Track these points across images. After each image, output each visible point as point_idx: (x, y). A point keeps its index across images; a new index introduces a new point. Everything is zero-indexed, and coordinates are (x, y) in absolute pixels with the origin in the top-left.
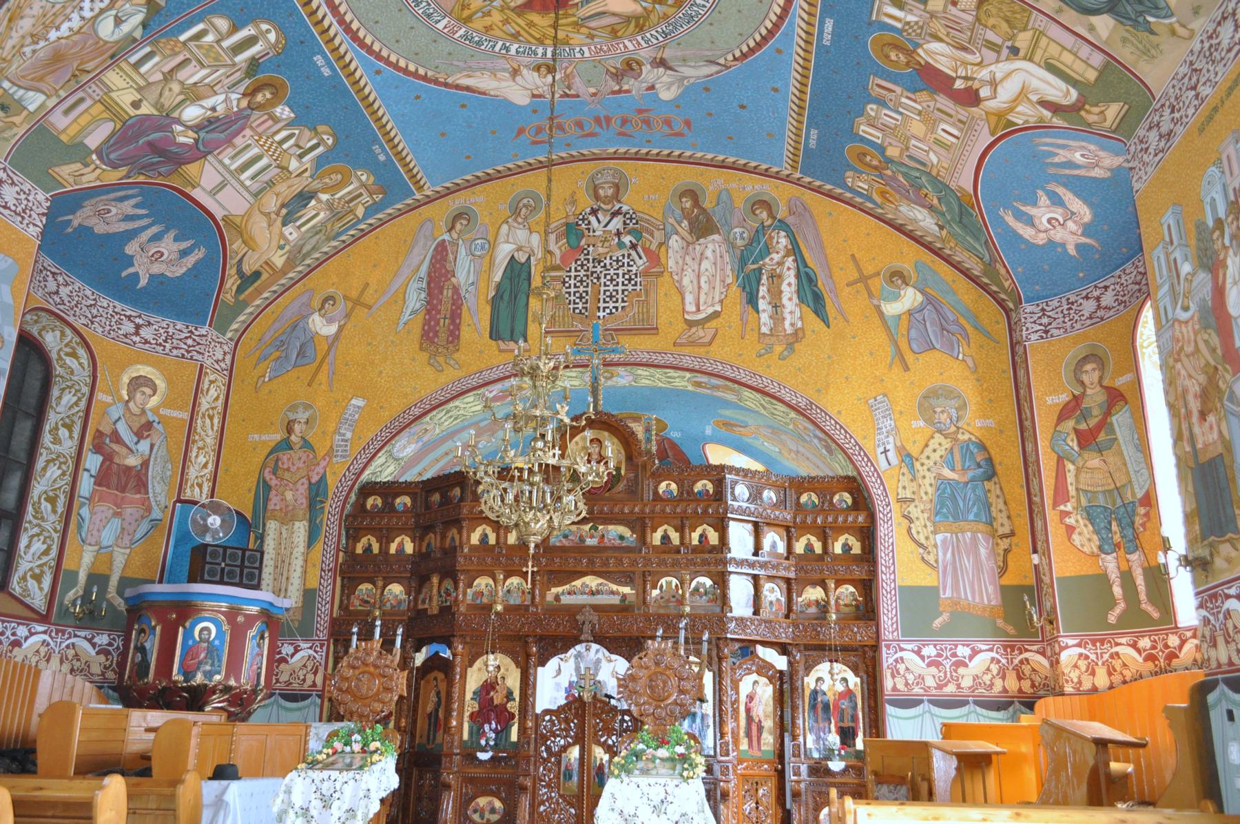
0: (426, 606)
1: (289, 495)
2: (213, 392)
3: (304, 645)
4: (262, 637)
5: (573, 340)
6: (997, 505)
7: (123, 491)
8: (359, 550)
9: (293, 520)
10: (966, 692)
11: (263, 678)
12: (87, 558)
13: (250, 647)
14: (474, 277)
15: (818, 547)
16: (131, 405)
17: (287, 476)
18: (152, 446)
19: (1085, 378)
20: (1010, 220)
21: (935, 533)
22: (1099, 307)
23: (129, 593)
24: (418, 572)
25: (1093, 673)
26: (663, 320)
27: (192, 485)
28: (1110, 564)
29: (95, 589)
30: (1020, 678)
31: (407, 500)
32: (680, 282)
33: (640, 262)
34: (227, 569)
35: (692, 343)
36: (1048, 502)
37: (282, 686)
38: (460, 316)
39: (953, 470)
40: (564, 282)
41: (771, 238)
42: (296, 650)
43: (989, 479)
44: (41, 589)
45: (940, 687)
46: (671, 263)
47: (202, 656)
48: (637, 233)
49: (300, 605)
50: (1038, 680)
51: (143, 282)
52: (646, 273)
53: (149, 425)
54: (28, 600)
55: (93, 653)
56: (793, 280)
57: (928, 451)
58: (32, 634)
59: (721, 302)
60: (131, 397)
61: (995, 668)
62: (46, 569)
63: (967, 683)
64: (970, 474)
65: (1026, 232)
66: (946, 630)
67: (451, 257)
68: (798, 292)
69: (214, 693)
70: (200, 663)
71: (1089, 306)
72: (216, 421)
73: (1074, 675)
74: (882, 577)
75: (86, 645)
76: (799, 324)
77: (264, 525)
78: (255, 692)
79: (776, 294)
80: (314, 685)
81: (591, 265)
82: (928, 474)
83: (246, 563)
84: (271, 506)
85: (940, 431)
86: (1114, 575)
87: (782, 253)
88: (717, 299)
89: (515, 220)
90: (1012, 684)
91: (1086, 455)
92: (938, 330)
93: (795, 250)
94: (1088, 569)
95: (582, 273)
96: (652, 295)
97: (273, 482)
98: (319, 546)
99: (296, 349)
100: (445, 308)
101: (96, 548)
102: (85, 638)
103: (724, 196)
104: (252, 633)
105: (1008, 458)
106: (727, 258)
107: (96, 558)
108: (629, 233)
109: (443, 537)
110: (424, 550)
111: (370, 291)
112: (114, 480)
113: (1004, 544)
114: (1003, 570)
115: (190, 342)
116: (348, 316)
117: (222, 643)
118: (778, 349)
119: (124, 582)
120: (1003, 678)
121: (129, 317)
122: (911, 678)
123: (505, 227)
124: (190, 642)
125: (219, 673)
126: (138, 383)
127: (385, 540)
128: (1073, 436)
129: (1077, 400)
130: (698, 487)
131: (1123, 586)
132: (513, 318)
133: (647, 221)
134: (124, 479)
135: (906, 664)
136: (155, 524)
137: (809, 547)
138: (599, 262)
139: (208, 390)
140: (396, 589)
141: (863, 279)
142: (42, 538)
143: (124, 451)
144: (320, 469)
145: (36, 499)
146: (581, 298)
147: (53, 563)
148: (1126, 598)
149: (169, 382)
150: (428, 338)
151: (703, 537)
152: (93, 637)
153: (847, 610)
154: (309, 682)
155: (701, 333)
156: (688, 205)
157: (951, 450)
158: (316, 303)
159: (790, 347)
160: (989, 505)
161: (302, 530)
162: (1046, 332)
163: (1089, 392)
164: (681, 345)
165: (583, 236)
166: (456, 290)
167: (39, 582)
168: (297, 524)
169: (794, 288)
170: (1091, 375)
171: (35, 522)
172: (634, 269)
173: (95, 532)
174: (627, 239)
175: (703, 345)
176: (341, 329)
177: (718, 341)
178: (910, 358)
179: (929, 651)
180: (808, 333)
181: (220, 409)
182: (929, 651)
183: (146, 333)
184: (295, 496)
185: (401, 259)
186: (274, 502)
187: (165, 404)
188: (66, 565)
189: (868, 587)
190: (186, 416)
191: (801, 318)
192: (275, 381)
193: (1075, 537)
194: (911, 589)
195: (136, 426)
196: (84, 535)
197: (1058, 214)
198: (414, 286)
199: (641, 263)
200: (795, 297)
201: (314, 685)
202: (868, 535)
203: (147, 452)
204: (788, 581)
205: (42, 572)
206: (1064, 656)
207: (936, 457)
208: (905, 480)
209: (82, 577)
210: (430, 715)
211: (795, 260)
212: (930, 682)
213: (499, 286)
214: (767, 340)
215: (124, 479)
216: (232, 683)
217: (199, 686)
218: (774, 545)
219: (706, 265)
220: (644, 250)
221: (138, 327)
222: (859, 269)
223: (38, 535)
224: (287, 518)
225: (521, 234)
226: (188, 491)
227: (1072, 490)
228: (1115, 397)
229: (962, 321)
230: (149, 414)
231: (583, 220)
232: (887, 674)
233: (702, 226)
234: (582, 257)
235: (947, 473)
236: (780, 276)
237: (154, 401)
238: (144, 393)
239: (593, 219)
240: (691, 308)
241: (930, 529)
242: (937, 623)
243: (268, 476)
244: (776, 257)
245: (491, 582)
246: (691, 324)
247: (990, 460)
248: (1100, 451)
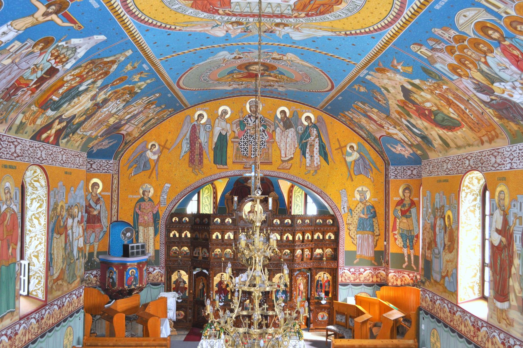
0: (197, 255)
1: (146, 218)
2: (115, 182)
3: (156, 268)
5: (243, 166)
6: (376, 226)
8: (171, 236)
9: (148, 226)
10: (362, 282)
14: (207, 141)
15: (321, 237)
17: (144, 211)
18: (101, 206)
19: (405, 194)
20: (389, 146)
21: (357, 234)
22: (412, 174)
23: (101, 257)
24: (193, 243)
25: (397, 281)
26: (274, 159)
28: (405, 251)
30: (377, 278)
31: (187, 219)
32: (280, 145)
33: (266, 137)
35: (283, 169)
36: (390, 230)
38: (202, 154)
39: (364, 214)
40: (239, 144)
41: (311, 131)
42: (154, 270)
43: (374, 217)
45: (354, 280)
46: (277, 138)
48: (264, 126)
50: (382, 278)
51: (94, 152)
52: (268, 142)
56: (318, 147)
57: (357, 208)
59: (294, 154)
61: (370, 275)
63: (362, 279)
64: (369, 216)
65: (394, 150)
66: (357, 264)
67: (198, 131)
68: (319, 152)
71: (409, 172)
73: (392, 281)
74: (340, 248)
76: (319, 163)
79: (312, 152)
80: (162, 280)
81: (249, 137)
82: (356, 216)
84: (140, 221)
85: (361, 202)
86: (406, 254)
87: (315, 137)
88: (292, 153)
89: (221, 118)
90: (375, 279)
91: (403, 218)
92: (363, 167)
93: (319, 136)
94: (399, 251)
95: (246, 140)
96: (270, 150)
97: (140, 213)
98: (158, 236)
99: (142, 164)
100: (197, 151)
103: (295, 114)
105: (381, 211)
106: (296, 137)
108: (262, 126)
109: (202, 234)
110: (194, 236)
111: (168, 143)
112: (91, 220)
113: (377, 238)
114: (376, 246)
115: (108, 166)
116: (161, 152)
118: (312, 172)
119: (99, 253)
120: (373, 278)
121: (88, 162)
122: (346, 278)
123: (217, 120)
126: (95, 185)
127: (180, 233)
128: (400, 211)
129: (402, 200)
130: (286, 221)
131: (408, 258)
132: (222, 156)
133: (268, 122)
135: (345, 273)
136: (105, 233)
137: (318, 237)
138: (252, 136)
140: (186, 249)
141: (341, 148)
143: (93, 209)
144: (156, 209)
146: (245, 150)
148: (408, 261)
150: (192, 162)
151: (287, 237)
153: (329, 256)
154: (160, 280)
155: (287, 165)
156: (283, 116)
157: (364, 209)
158: (149, 147)
159: (316, 171)
160: (373, 226)
162: (396, 176)
163: (406, 199)
164: (280, 169)
165: (246, 126)
166: (200, 144)
168: (150, 228)
169: (318, 150)
170: (407, 194)
172: (264, 140)
174: (262, 128)
175: (287, 169)
176: (159, 157)
177: (292, 168)
178: (353, 176)
179: (352, 270)
180: (322, 167)
182: (352, 270)
183: (94, 166)
184: (148, 218)
185: (179, 132)
186: (141, 219)
187: (102, 191)
189: (336, 250)
190: (110, 194)
191: (320, 161)
192: (136, 176)
193: (397, 241)
194: (349, 251)
195: (95, 200)
197: (403, 149)
198: (185, 142)
199: (266, 138)
200: (318, 153)
201: (162, 280)
202: (337, 234)
204: (312, 248)
206: (390, 275)
207: (359, 210)
208: (349, 217)
210: (201, 290)
211: (319, 140)
212: (352, 279)
213: (216, 144)
214: (308, 169)
218: (308, 237)
219: (289, 139)
220: (268, 133)
221: (91, 165)
222: (340, 145)
224: (146, 225)
225: (223, 123)
227: (398, 228)
228: (413, 204)
229: (371, 165)
230: (98, 195)
231: (246, 119)
232: (340, 276)
233: (288, 123)
234: (246, 134)
235: (362, 216)
236: (313, 145)
239: (249, 119)
240: (283, 155)
241: (356, 233)
242: (355, 262)
244: (312, 138)
245: (219, 250)
246: (283, 161)
247: (375, 212)
248: (407, 218)
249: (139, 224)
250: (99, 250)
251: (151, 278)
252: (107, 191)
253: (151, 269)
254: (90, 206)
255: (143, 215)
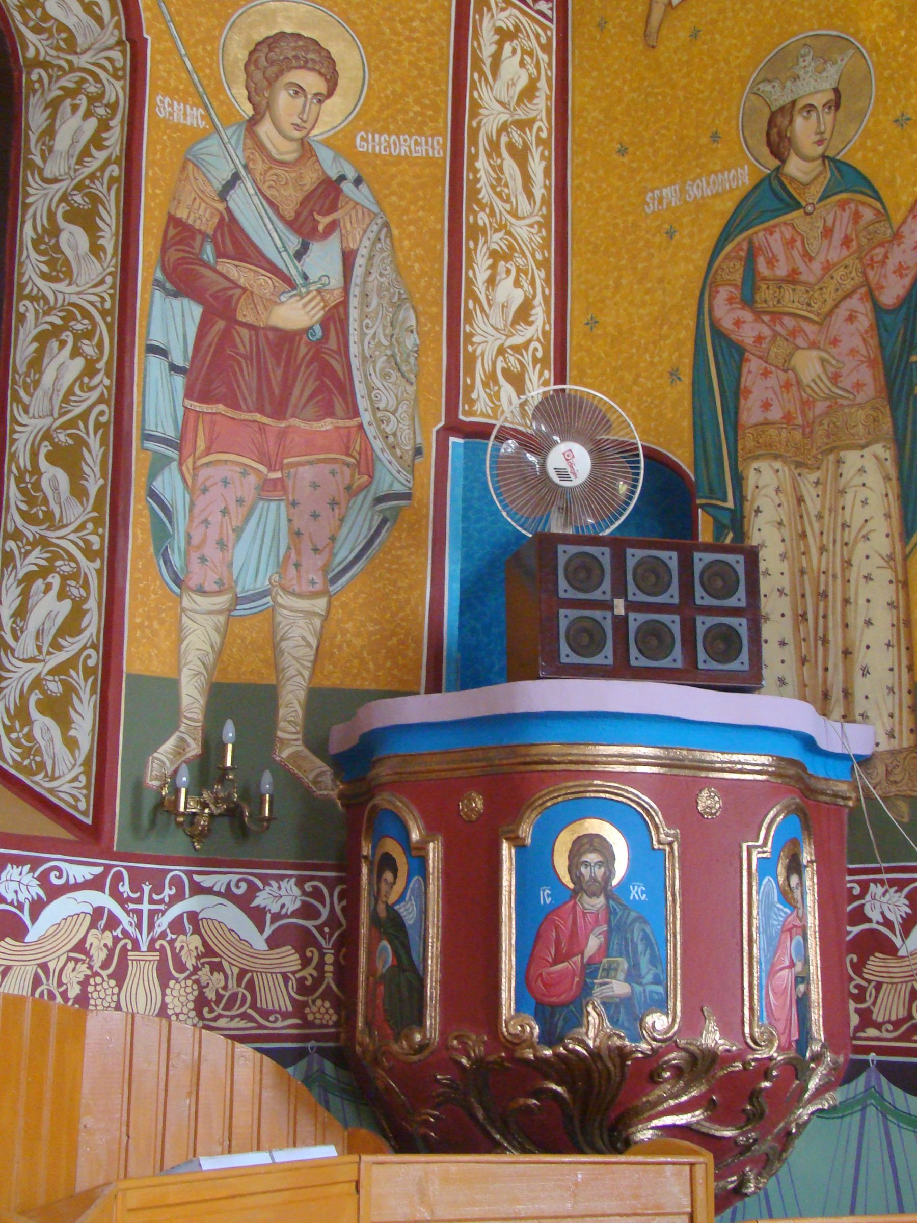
1: (808, 365)
4: (795, 866)
7: (279, 411)
9: (835, 445)
11: (816, 1015)
12: (200, 636)
13: (760, 902)
16: (265, 130)
18: (348, 258)
23: (341, 738)
27: (491, 378)
29: (229, 732)
34: (636, 620)
37: (887, 1036)
44: (71, 744)
47: (593, 944)
49: (907, 740)
53: (329, 192)
54: (39, 783)
55: (259, 942)
58: (54, 892)
60: (261, 110)
62: (76, 677)
69: (653, 1079)
70: (590, 969)
72: (537, 167)
75: (233, 917)
77: (739, 481)
78: (797, 1069)
83: (701, 597)
84: (751, 413)
101: (222, 600)
102: (228, 894)
104: (759, 848)
107: (225, 632)
112: (248, 377)
117: (658, 890)
119: (324, 704)
124: (545, 896)
125: (662, 1006)
134: (276, 376)
139: (497, 59)
142: (55, 580)
143: (263, 282)
145: (24, 460)
147: (94, 659)
149: (373, 43)
152: (253, 890)
161: (874, 478)
167: (65, 723)
168: (852, 458)
171: (31, 532)
173: (211, 550)
181: (544, 127)
187: (369, 118)
188: (136, 658)
190: (437, 147)
195: (291, 199)
196: (177, 561)
203: (336, 281)
205: (70, 689)
209: (192, 697)
215: (276, 376)
216: (712, 1038)
217: (595, 1054)
223: (43, 572)
224: (813, 444)
226: (479, 393)
230: (325, 155)
237: (335, 113)
238: (299, 90)
243: (726, 314)
249: (747, 442)
250: (334, 679)
251: (889, 1006)
252: (418, 127)
253: (886, 905)
254: (234, 240)
255: (778, 351)
